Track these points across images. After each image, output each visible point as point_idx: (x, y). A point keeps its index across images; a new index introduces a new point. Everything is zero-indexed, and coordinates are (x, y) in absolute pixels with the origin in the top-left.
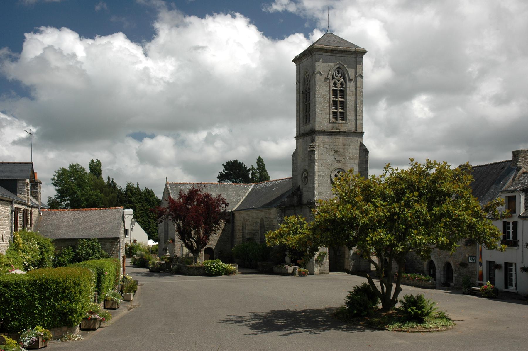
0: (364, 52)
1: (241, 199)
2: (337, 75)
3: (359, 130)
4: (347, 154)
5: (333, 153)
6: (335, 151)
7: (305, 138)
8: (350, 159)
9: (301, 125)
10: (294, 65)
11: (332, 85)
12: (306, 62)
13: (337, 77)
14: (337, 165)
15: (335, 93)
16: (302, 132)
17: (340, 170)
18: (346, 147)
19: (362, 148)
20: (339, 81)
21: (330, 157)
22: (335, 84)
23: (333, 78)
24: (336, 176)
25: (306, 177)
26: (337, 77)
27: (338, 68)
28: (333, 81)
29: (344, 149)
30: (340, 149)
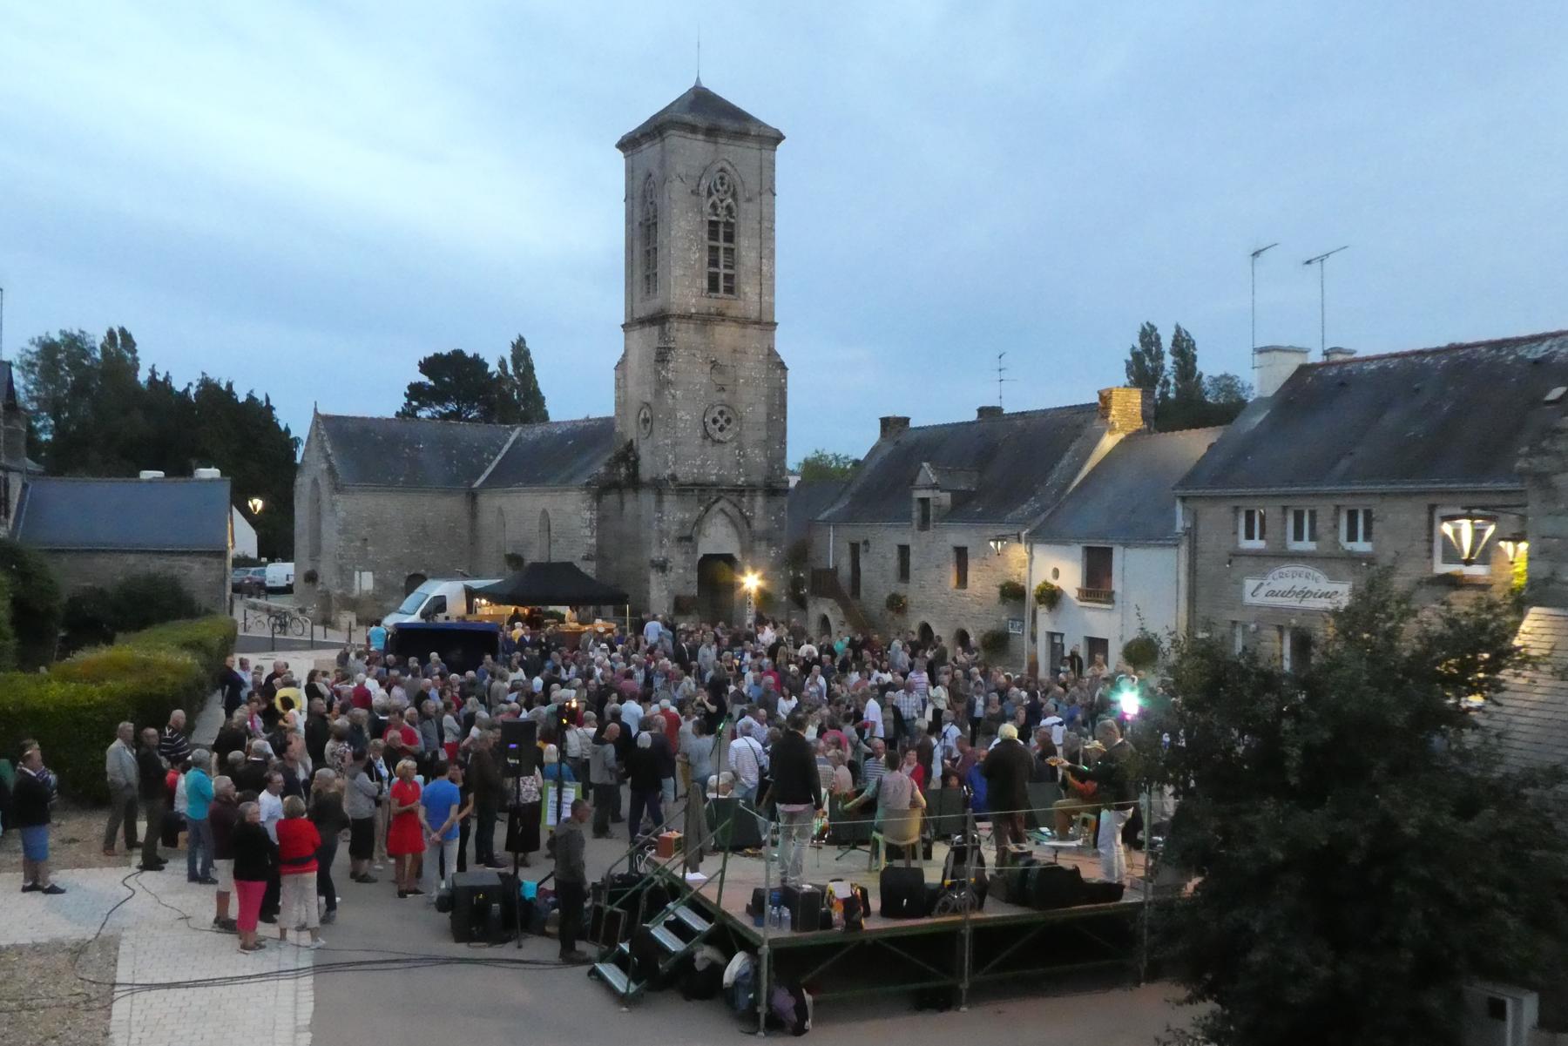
0: (778, 138)
1: (490, 462)
3: (766, 318)
5: (707, 369)
6: (714, 364)
7: (647, 329)
9: (637, 298)
10: (620, 154)
11: (707, 208)
12: (650, 151)
16: (636, 316)
21: (701, 377)
22: (714, 206)
23: (710, 194)
24: (715, 421)
25: (646, 421)
27: (722, 170)
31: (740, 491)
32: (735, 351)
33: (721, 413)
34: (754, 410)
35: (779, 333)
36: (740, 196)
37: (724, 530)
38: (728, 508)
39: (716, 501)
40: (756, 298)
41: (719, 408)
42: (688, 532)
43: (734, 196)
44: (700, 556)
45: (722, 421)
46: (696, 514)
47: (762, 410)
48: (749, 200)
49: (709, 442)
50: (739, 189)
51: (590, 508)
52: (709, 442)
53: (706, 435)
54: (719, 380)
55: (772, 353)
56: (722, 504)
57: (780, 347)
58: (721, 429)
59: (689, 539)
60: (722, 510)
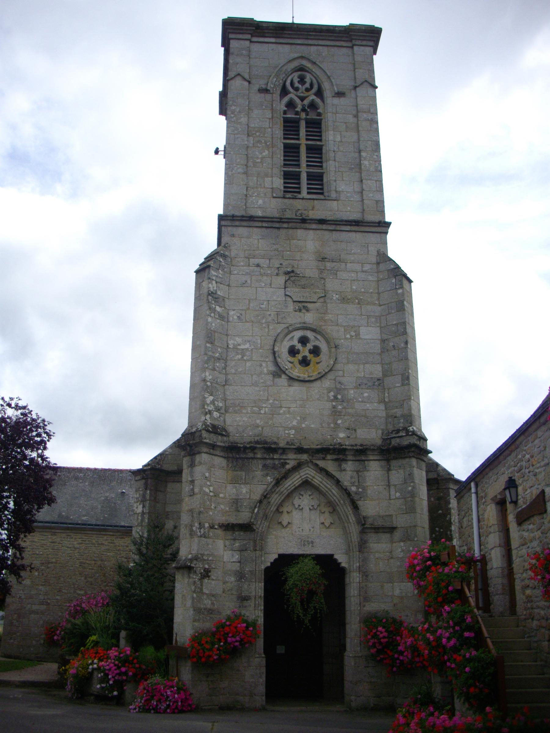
2: (297, 85)
3: (370, 217)
4: (331, 284)
5: (281, 280)
8: (344, 300)
13: (297, 89)
14: (296, 319)
15: (290, 127)
17: (310, 335)
18: (328, 265)
19: (382, 267)
20: (302, 99)
24: (293, 352)
26: (297, 89)
28: (286, 99)
29: (321, 271)
30: (308, 266)
31: (339, 453)
32: (324, 259)
33: (304, 341)
34: (357, 332)
35: (392, 236)
36: (328, 93)
37: (317, 518)
38: (318, 479)
39: (298, 467)
40: (357, 197)
41: (298, 334)
42: (244, 517)
43: (320, 93)
44: (273, 557)
45: (305, 352)
46: (258, 490)
47: (370, 334)
48: (340, 94)
49: (283, 380)
50: (326, 86)
51: (143, 501)
52: (283, 380)
53: (279, 371)
54: (296, 293)
55: (383, 258)
56: (308, 472)
57: (395, 251)
58: (305, 362)
59: (247, 528)
60: (306, 484)
